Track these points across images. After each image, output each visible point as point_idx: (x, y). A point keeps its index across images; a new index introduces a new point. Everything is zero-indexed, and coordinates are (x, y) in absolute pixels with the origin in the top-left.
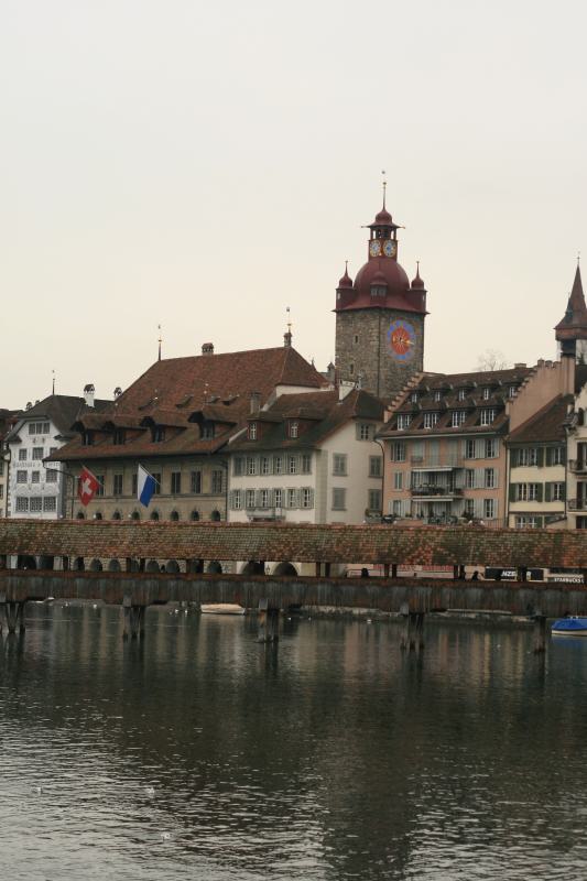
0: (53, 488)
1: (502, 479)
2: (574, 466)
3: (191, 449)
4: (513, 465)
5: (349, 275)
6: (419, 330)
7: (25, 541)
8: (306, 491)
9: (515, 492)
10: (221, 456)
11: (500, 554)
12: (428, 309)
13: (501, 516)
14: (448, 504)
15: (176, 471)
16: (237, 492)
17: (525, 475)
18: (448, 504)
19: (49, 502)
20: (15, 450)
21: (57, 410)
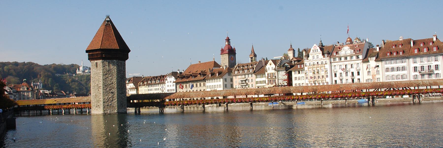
0: (174, 88)
1: (254, 80)
2: (267, 78)
3: (199, 79)
4: (257, 78)
5: (223, 48)
6: (235, 57)
7: (184, 96)
8: (220, 85)
9: (257, 83)
10: (204, 80)
11: (265, 92)
12: (236, 53)
13: (255, 87)
14: (245, 85)
15: (196, 83)
16: (208, 86)
17: (259, 79)
18: (245, 86)
19: (174, 90)
20: (166, 81)
21: (174, 74)
